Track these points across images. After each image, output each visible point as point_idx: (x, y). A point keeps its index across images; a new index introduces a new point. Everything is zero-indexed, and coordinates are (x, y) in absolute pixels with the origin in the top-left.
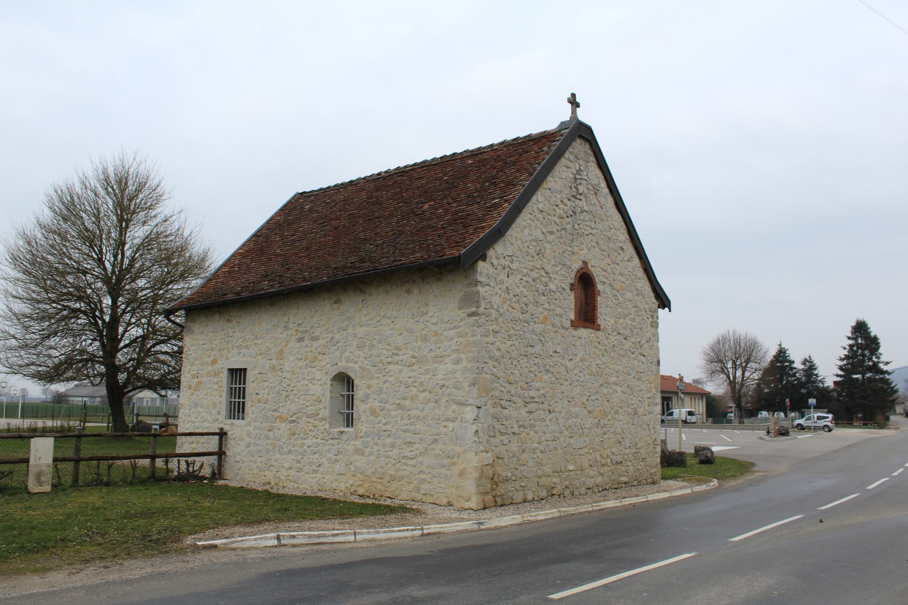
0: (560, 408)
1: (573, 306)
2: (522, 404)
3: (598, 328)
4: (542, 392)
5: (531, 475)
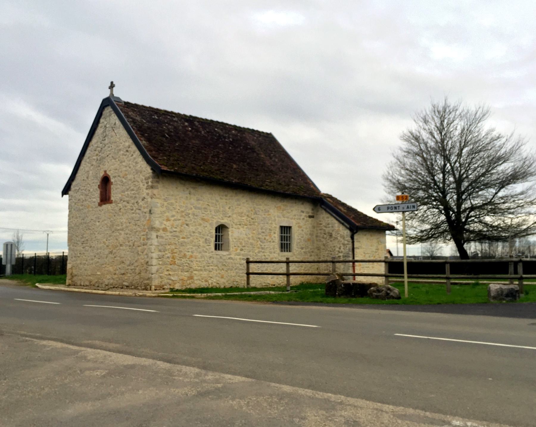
0: (94, 245)
1: (99, 196)
2: (81, 245)
3: (111, 202)
4: (87, 238)
5: (83, 275)
